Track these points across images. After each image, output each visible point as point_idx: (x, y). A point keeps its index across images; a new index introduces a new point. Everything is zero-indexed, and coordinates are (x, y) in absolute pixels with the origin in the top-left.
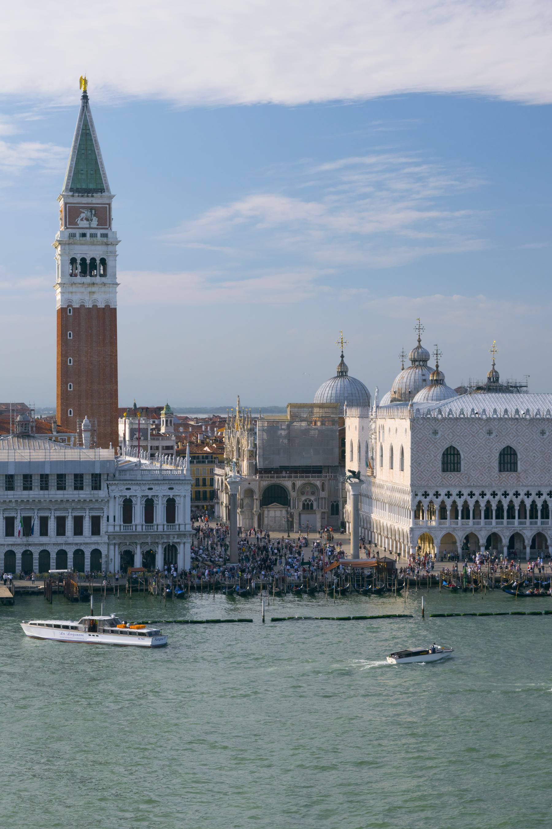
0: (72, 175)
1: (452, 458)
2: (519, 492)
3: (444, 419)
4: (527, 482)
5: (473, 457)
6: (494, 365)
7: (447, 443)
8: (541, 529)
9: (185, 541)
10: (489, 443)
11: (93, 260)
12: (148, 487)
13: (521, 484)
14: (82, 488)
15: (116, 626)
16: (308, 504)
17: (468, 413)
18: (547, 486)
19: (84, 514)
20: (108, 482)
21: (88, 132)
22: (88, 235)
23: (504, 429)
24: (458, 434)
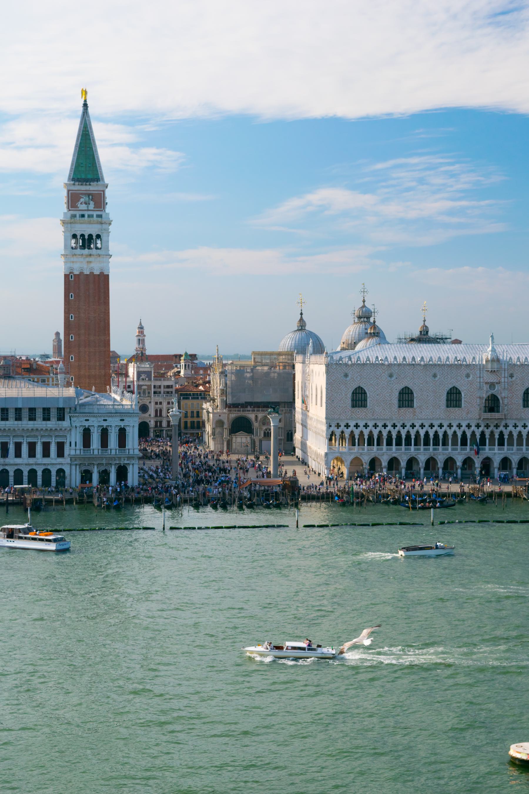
0: (74, 167)
2: (416, 424)
3: (353, 365)
5: (377, 395)
6: (425, 321)
8: (432, 455)
9: (134, 462)
11: (90, 236)
12: (103, 419)
14: (49, 419)
15: (28, 534)
16: (268, 432)
17: (373, 360)
18: (437, 419)
19: (51, 441)
20: (70, 415)
21: (87, 133)
22: (86, 216)
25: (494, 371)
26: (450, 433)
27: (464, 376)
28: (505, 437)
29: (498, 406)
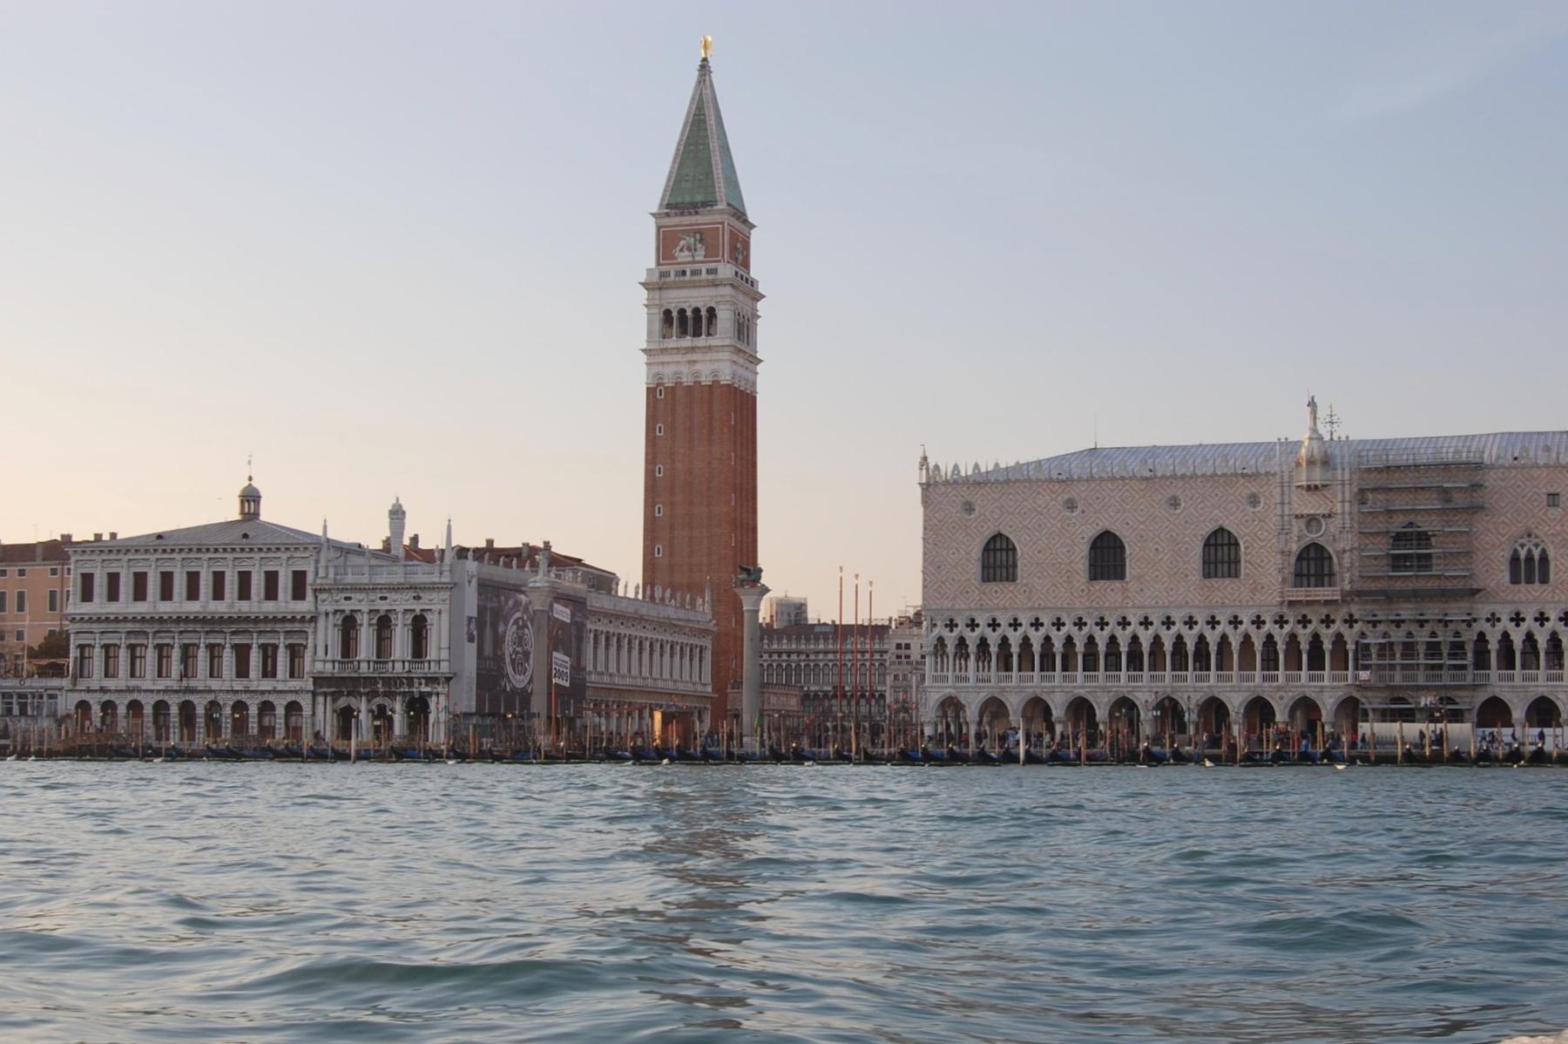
0: (671, 184)
1: (1004, 558)
2: (1130, 618)
4: (1142, 600)
5: (1039, 552)
7: (989, 527)
8: (1169, 690)
9: (440, 689)
10: (1069, 525)
11: (697, 311)
12: (379, 595)
13: (1131, 603)
18: (1179, 607)
19: (276, 642)
21: (702, 117)
22: (688, 273)
23: (1098, 498)
24: (1010, 510)
25: (1316, 487)
26: (1212, 638)
27: (1244, 501)
28: (1348, 647)
29: (1331, 574)
